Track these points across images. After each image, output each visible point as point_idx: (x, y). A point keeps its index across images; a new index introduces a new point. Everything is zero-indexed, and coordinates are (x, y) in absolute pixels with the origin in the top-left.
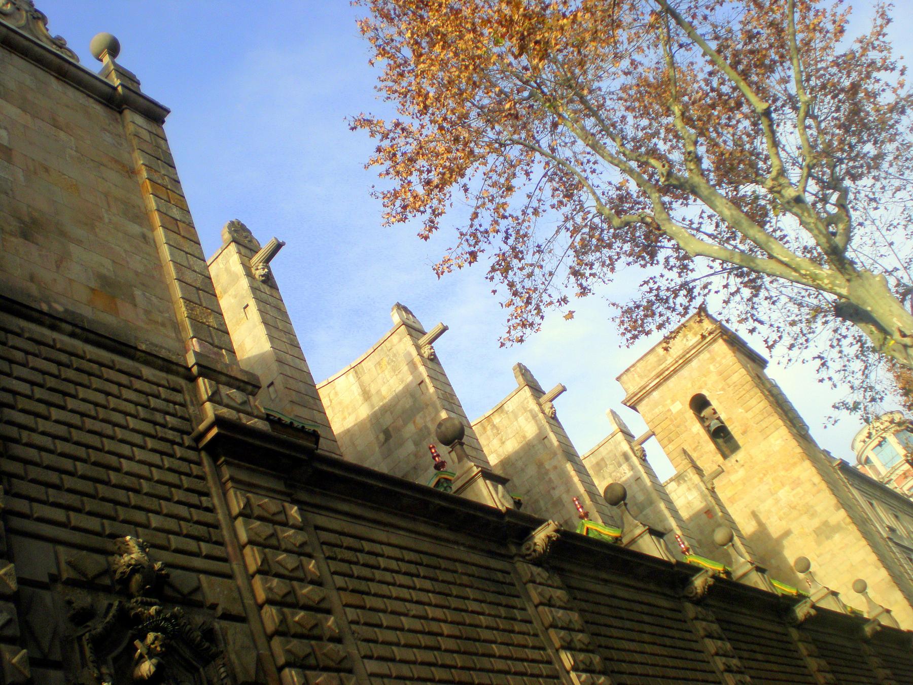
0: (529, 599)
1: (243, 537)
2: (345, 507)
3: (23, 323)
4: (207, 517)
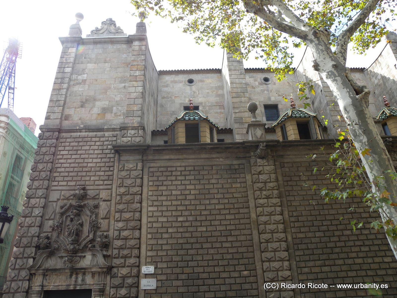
2: (167, 157)
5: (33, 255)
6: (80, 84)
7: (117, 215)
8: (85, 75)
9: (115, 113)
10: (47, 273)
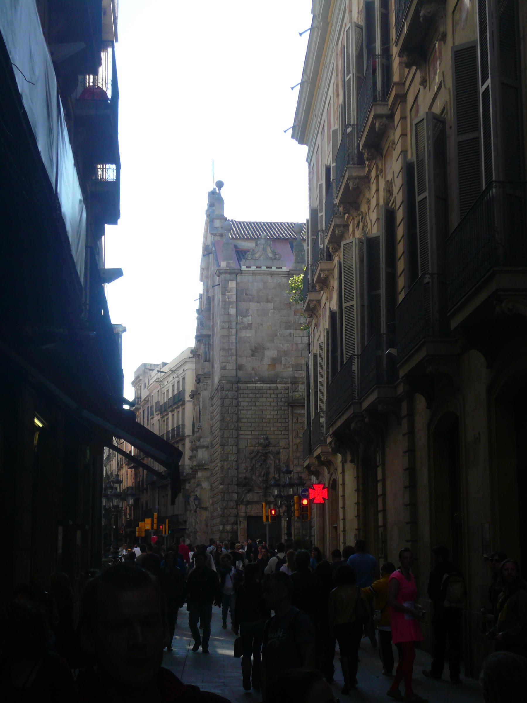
3: (249, 385)
5: (236, 491)
6: (246, 328)
7: (295, 462)
8: (250, 318)
9: (285, 365)
10: (248, 503)
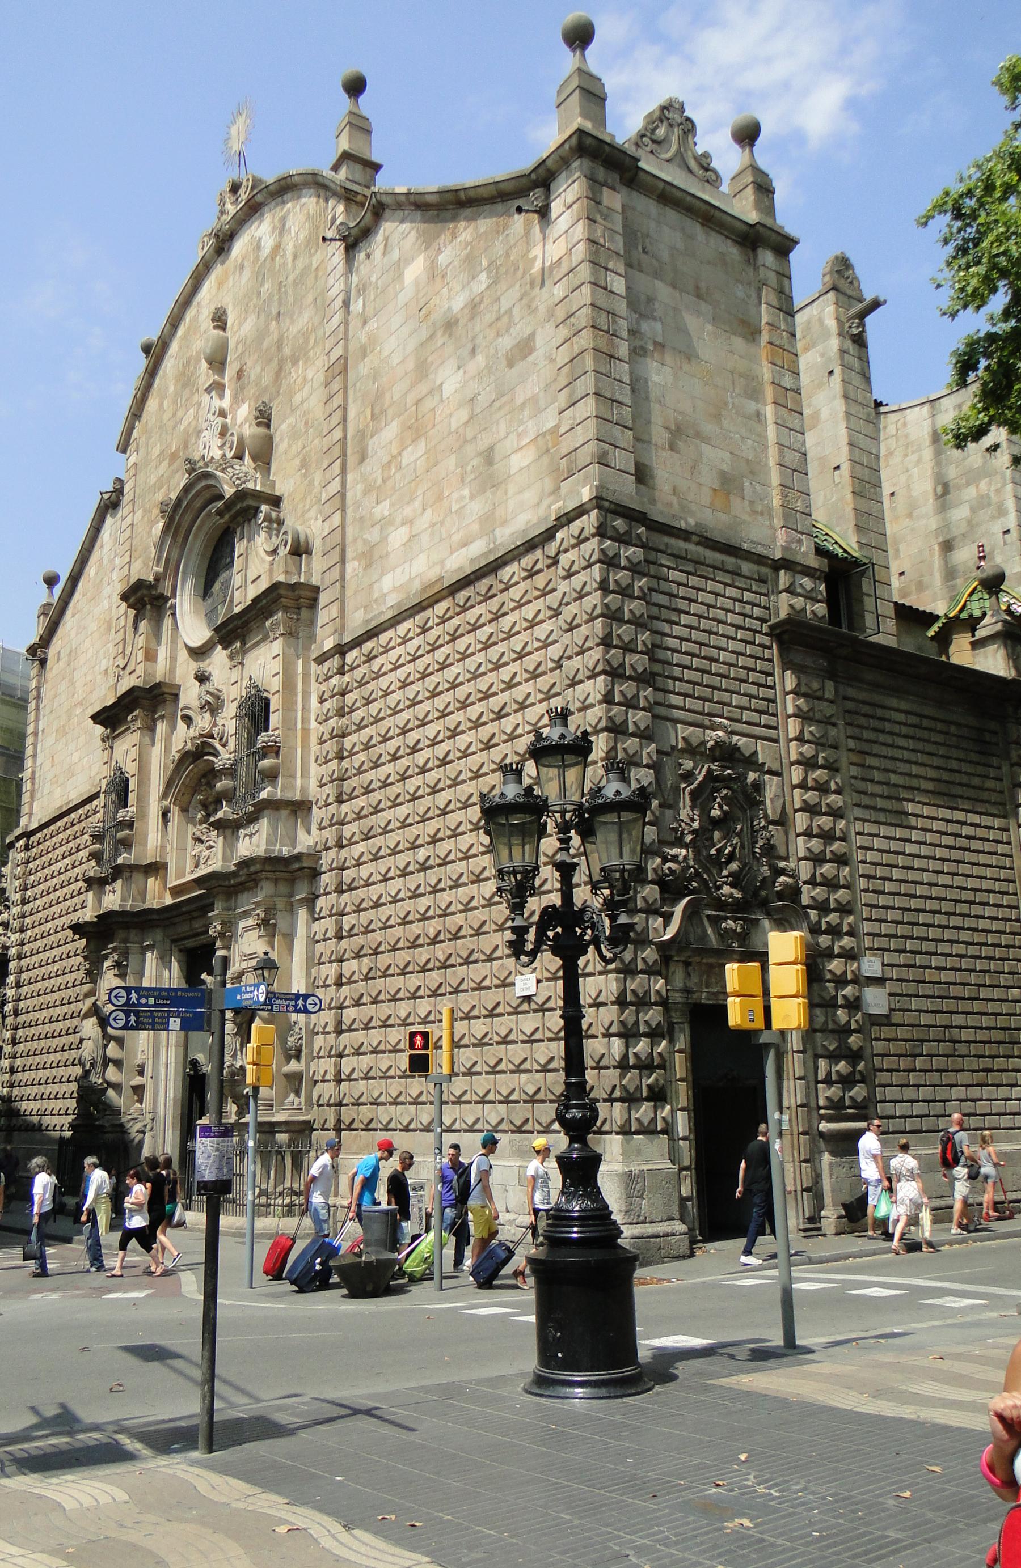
0: (1008, 757)
1: (790, 710)
3: (666, 539)
4: (769, 693)
